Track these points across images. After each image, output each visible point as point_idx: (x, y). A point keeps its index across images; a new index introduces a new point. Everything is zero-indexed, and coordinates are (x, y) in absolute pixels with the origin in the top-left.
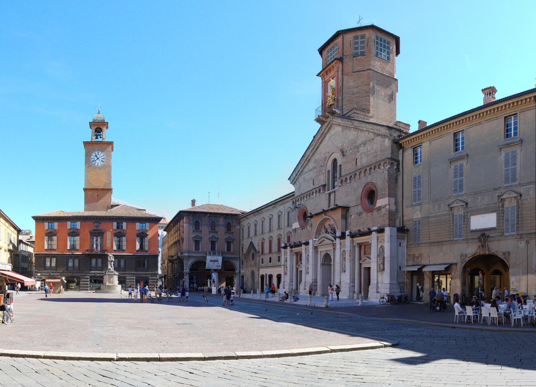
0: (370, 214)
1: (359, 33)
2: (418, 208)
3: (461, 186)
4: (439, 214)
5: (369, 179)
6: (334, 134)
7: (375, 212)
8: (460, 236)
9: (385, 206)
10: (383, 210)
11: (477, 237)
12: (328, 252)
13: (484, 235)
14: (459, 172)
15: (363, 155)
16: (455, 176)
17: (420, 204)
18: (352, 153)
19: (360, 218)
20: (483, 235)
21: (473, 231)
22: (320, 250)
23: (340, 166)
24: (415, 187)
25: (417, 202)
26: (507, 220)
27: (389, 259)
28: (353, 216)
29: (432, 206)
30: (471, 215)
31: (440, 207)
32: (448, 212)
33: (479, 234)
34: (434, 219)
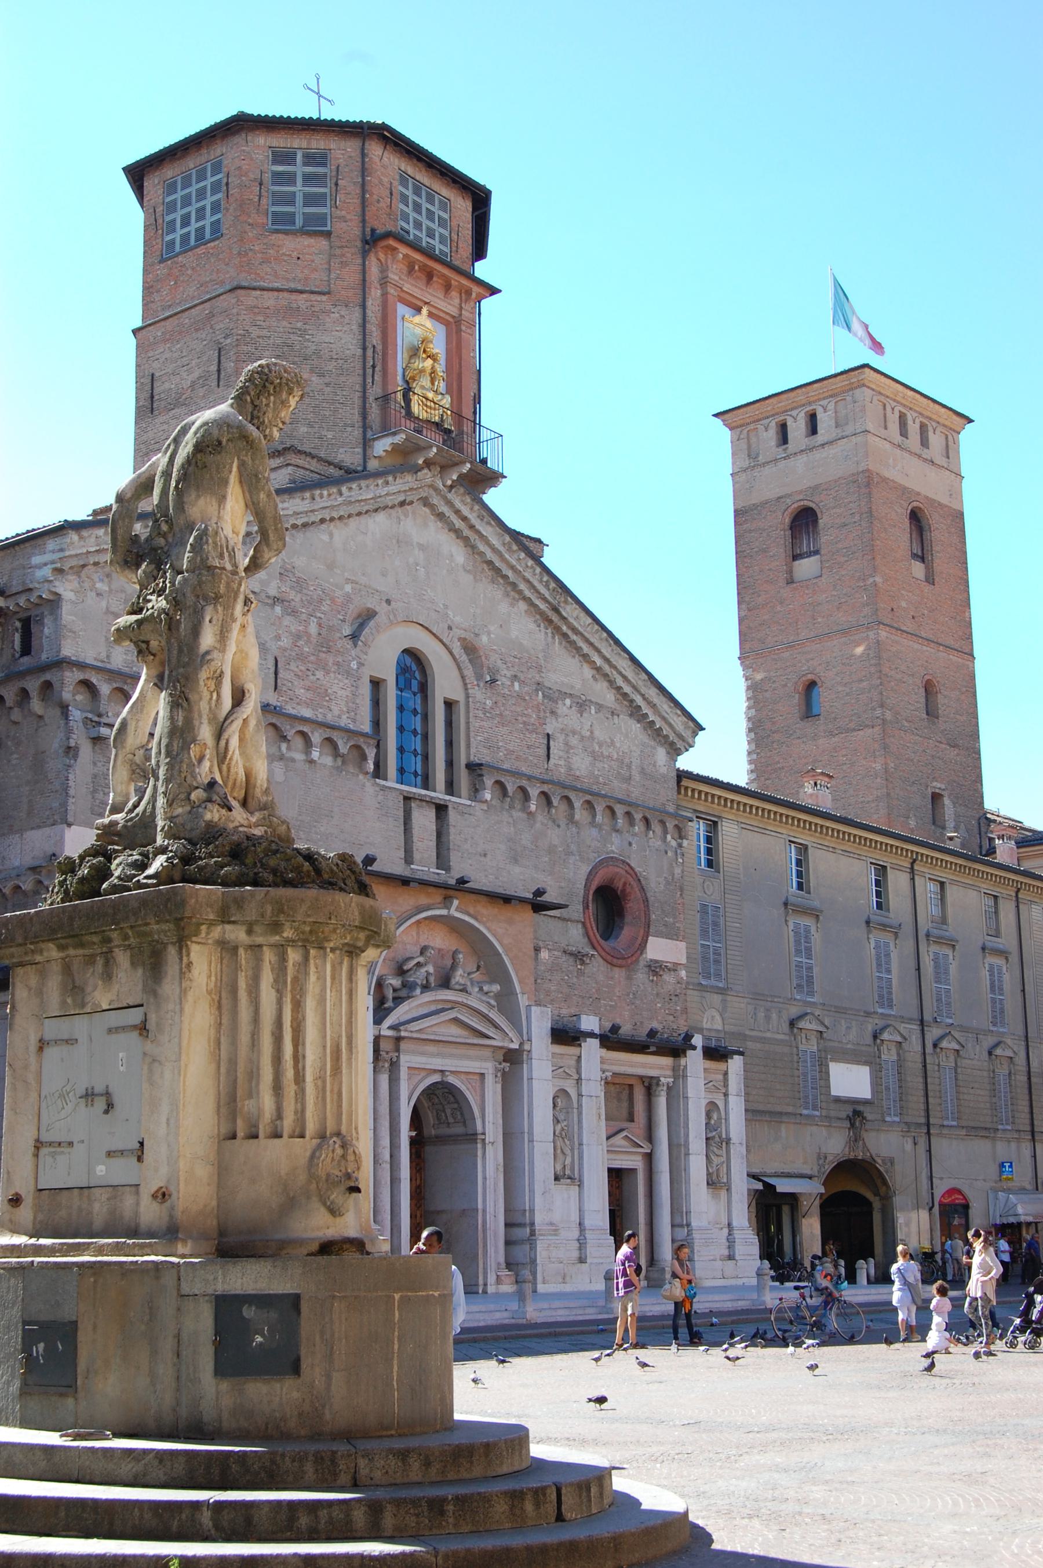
0: (619, 974)
1: (298, 142)
2: (717, 998)
3: (810, 980)
4: (768, 1035)
5: (615, 846)
6: (422, 547)
7: (641, 976)
8: (815, 1108)
9: (674, 968)
10: (669, 978)
11: (844, 1115)
12: (451, 1079)
13: (855, 1114)
14: (803, 943)
15: (574, 741)
16: (798, 952)
17: (722, 991)
18: (520, 697)
19: (581, 973)
20: (857, 1113)
21: (838, 1100)
22: (406, 1060)
23: (449, 705)
24: (704, 934)
25: (713, 982)
26: (888, 1088)
27: (743, 1150)
28: (544, 955)
29: (750, 1008)
30: (833, 1060)
31: (768, 1018)
32: (787, 1038)
33: (848, 1110)
34: (758, 1046)
